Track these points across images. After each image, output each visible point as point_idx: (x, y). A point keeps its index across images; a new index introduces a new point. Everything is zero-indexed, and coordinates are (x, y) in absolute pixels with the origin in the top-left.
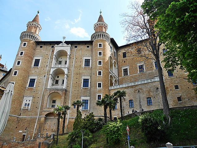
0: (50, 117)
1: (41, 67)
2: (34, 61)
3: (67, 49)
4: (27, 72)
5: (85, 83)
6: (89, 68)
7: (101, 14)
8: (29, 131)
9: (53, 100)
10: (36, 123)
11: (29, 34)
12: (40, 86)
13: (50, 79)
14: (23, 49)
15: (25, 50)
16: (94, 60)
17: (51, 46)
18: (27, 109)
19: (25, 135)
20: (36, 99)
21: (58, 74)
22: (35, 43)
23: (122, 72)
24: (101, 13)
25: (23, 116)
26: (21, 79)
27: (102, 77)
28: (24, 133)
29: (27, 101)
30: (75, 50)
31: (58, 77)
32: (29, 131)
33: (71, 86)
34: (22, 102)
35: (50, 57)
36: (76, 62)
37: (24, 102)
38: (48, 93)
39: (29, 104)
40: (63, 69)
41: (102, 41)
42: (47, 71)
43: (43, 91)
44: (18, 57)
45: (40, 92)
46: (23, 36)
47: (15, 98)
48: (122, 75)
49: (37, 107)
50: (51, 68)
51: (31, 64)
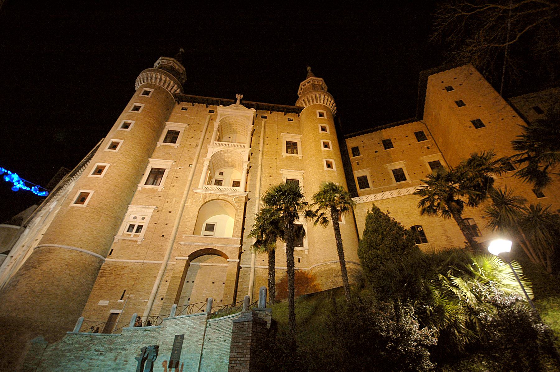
0: (200, 262)
12: (176, 184)
16: (311, 140)
17: (208, 109)
18: (135, 239)
25: (117, 257)
27: (336, 174)
28: (113, 308)
29: (135, 218)
30: (263, 122)
31: (221, 173)
35: (205, 129)
37: (128, 220)
39: (140, 227)
45: (174, 199)
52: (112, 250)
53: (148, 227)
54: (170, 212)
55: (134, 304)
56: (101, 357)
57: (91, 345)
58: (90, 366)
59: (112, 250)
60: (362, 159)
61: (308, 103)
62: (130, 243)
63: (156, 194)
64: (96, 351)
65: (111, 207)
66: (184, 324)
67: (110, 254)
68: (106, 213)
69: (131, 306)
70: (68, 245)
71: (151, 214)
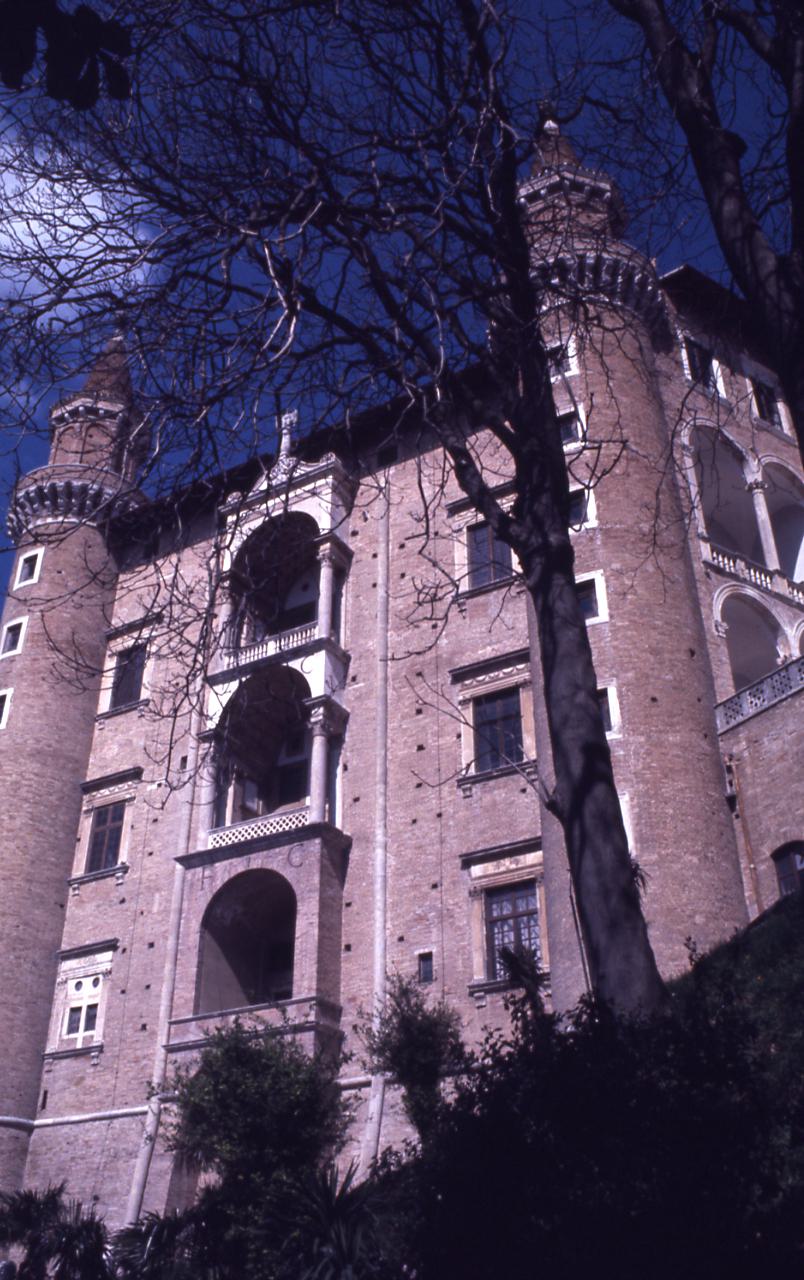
12: (156, 845)
20: (139, 957)
25: (58, 1113)
26: (18, 822)
29: (79, 985)
39: (92, 1008)
40: (295, 664)
49: (144, 1027)
52: (46, 1093)
53: (109, 1008)
59: (46, 1093)
65: (8, 979)
67: (44, 1106)
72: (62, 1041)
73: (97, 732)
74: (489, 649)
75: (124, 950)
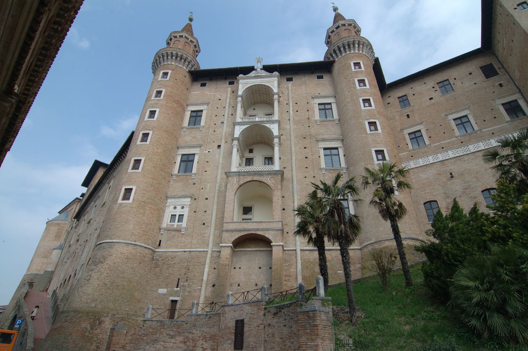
0: (243, 247)
1: (206, 126)
2: (188, 114)
3: (273, 82)
4: (173, 134)
5: (329, 157)
6: (334, 121)
7: (339, 11)
8: (188, 289)
9: (244, 207)
10: (207, 266)
11: (174, 53)
12: (207, 169)
13: (235, 150)
14: (161, 84)
15: (165, 86)
16: (348, 100)
19: (176, 301)
21: (251, 145)
22: (188, 75)
23: (405, 139)
24: (335, 9)
25: (166, 247)
26: (159, 151)
28: (171, 295)
29: (175, 208)
31: (251, 151)
32: (188, 289)
33: (294, 166)
34: (164, 211)
35: (227, 104)
36: (295, 110)
37: (169, 211)
38: (234, 182)
39: (181, 216)
40: (268, 125)
41: (359, 56)
42: (224, 134)
43: (218, 181)
44: (152, 102)
45: (209, 185)
46: (161, 59)
47: (144, 199)
48: (408, 148)
50: (235, 124)
51: (182, 120)
52: (160, 241)
53: (189, 216)
54: (207, 199)
55: (189, 292)
56: (173, 340)
57: (162, 330)
58: (164, 348)
59: (160, 241)
60: (412, 111)
61: (339, 54)
62: (174, 233)
63: (190, 181)
64: (167, 335)
66: (242, 310)
67: (159, 245)
68: (150, 206)
69: (187, 294)
70: (124, 240)
71: (189, 203)
72: (167, 225)
73: (182, 132)
74: (328, 136)
75: (195, 199)
